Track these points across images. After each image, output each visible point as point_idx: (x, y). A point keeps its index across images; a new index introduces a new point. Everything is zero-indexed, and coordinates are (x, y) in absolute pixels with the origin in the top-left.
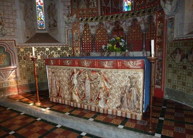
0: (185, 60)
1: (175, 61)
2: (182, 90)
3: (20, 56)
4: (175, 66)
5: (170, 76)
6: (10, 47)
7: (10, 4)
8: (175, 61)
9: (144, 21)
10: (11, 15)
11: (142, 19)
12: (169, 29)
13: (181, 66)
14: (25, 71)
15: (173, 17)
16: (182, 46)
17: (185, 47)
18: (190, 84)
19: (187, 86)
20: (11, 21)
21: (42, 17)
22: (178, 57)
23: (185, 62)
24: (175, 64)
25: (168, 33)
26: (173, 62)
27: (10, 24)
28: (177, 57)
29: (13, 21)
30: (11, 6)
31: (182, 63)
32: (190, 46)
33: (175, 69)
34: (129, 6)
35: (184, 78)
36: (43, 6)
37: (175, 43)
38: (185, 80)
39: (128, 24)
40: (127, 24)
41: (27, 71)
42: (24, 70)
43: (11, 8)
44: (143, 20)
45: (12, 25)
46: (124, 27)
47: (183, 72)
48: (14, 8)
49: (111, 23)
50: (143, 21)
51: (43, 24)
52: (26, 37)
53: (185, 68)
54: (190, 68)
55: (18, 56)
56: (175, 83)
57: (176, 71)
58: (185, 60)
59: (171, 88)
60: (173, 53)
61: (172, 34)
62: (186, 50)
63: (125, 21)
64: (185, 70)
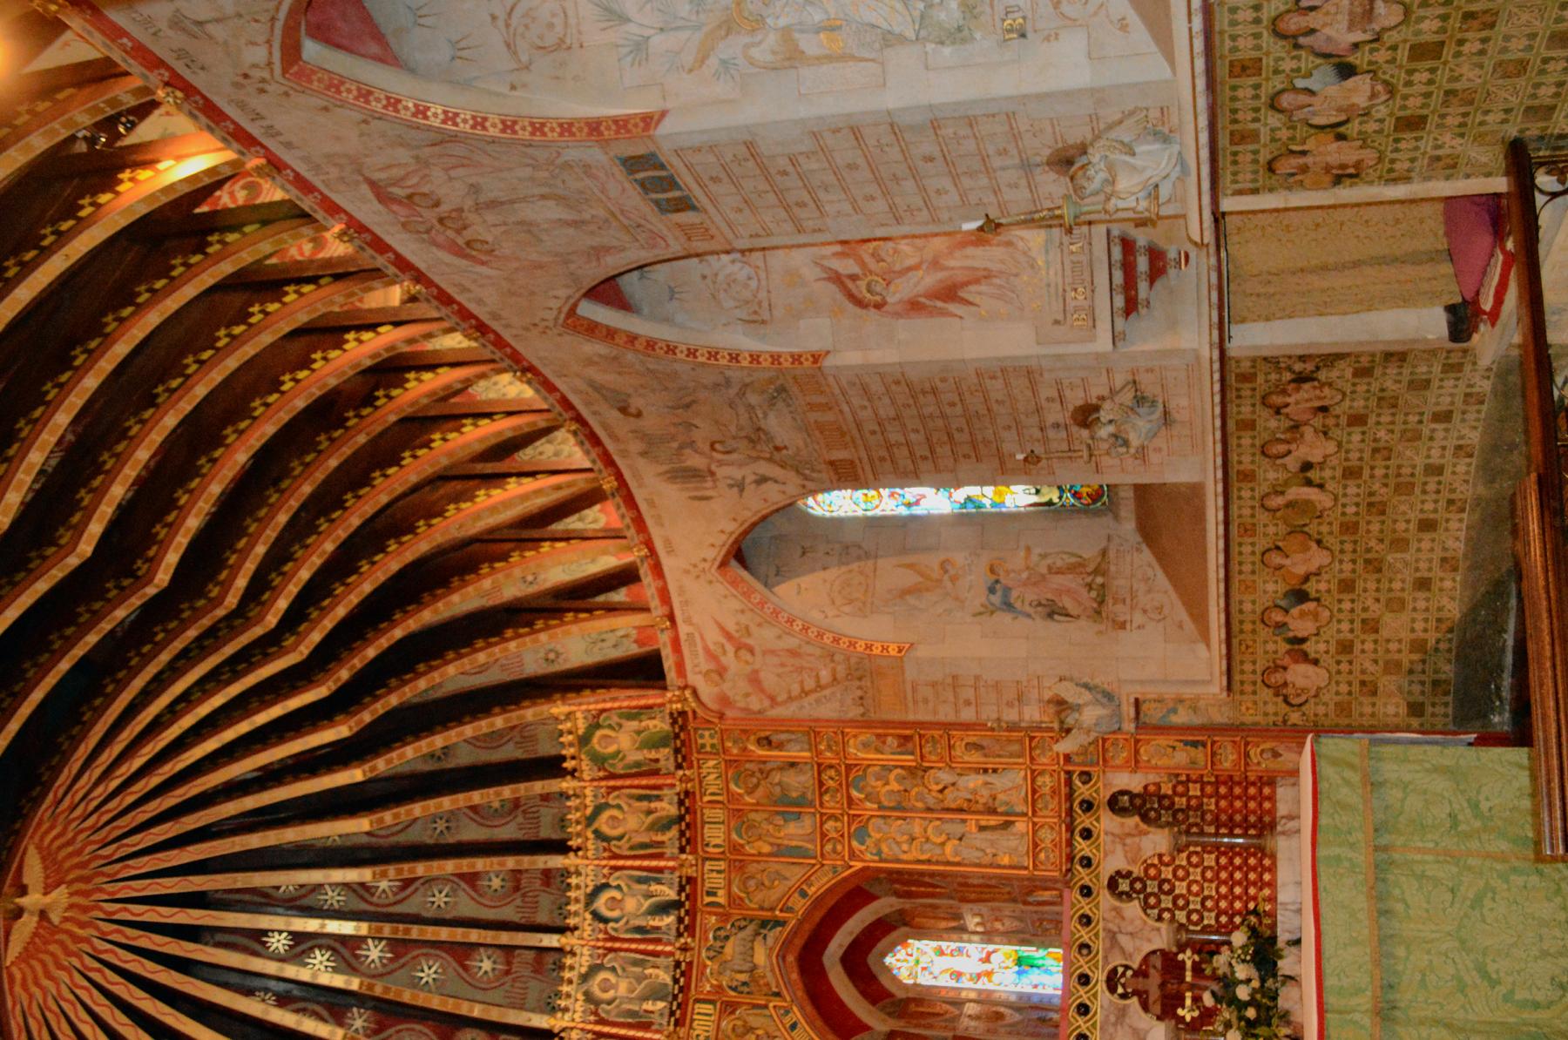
0: (1309, 647)
1: (1319, 689)
2: (1449, 650)
4: (1344, 688)
5: (1391, 710)
8: (1319, 689)
9: (1129, 835)
11: (1119, 848)
12: (1182, 717)
13: (1338, 663)
15: (1132, 700)
16: (1254, 663)
17: (1260, 651)
18: (1413, 620)
19: (1426, 630)
22: (1301, 676)
23: (1322, 647)
24: (1333, 688)
25: (1197, 720)
26: (1325, 697)
28: (1301, 682)
31: (1327, 660)
32: (1254, 631)
33: (1356, 688)
34: (1019, 961)
35: (1393, 646)
37: (1242, 692)
38: (1400, 641)
39: (1132, 922)
40: (1130, 929)
44: (1122, 838)
46: (1147, 948)
47: (1363, 651)
49: (1112, 1018)
50: (1128, 841)
53: (1346, 647)
54: (1345, 626)
56: (1423, 683)
57: (1363, 683)
58: (1309, 647)
59: (1450, 699)
60: (1286, 701)
61: (1202, 704)
62: (1271, 647)
63: (1112, 936)
64: (1358, 647)
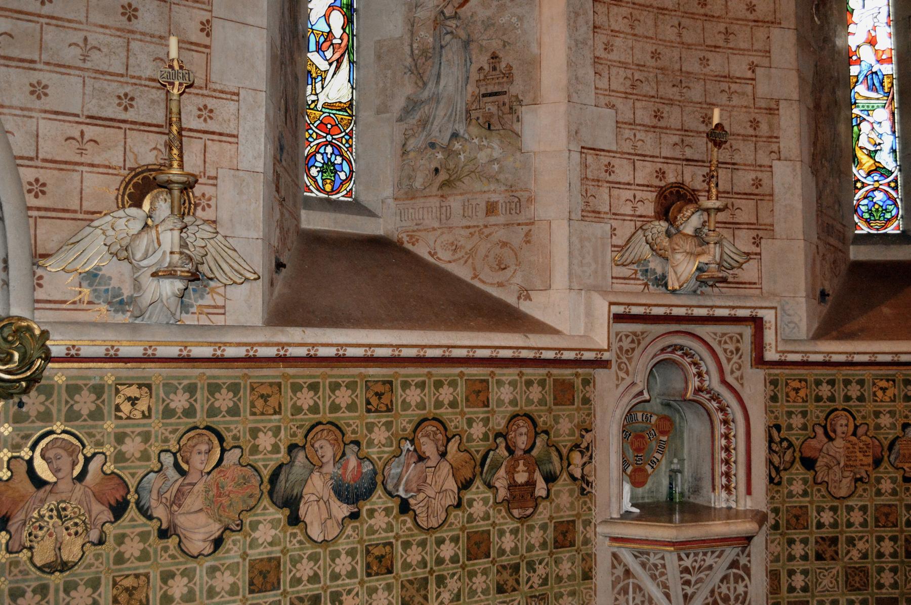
3: (784, 434)
6: (727, 368)
7: (745, 67)
10: (745, 137)
14: (805, 557)
20: (744, 180)
21: (886, 147)
27: (738, 202)
29: (758, 183)
30: (749, 74)
36: (889, 69)
41: (819, 557)
42: (798, 550)
43: (749, 89)
45: (745, 211)
48: (762, 89)
51: (889, 197)
52: (818, 293)
55: (771, 440)
